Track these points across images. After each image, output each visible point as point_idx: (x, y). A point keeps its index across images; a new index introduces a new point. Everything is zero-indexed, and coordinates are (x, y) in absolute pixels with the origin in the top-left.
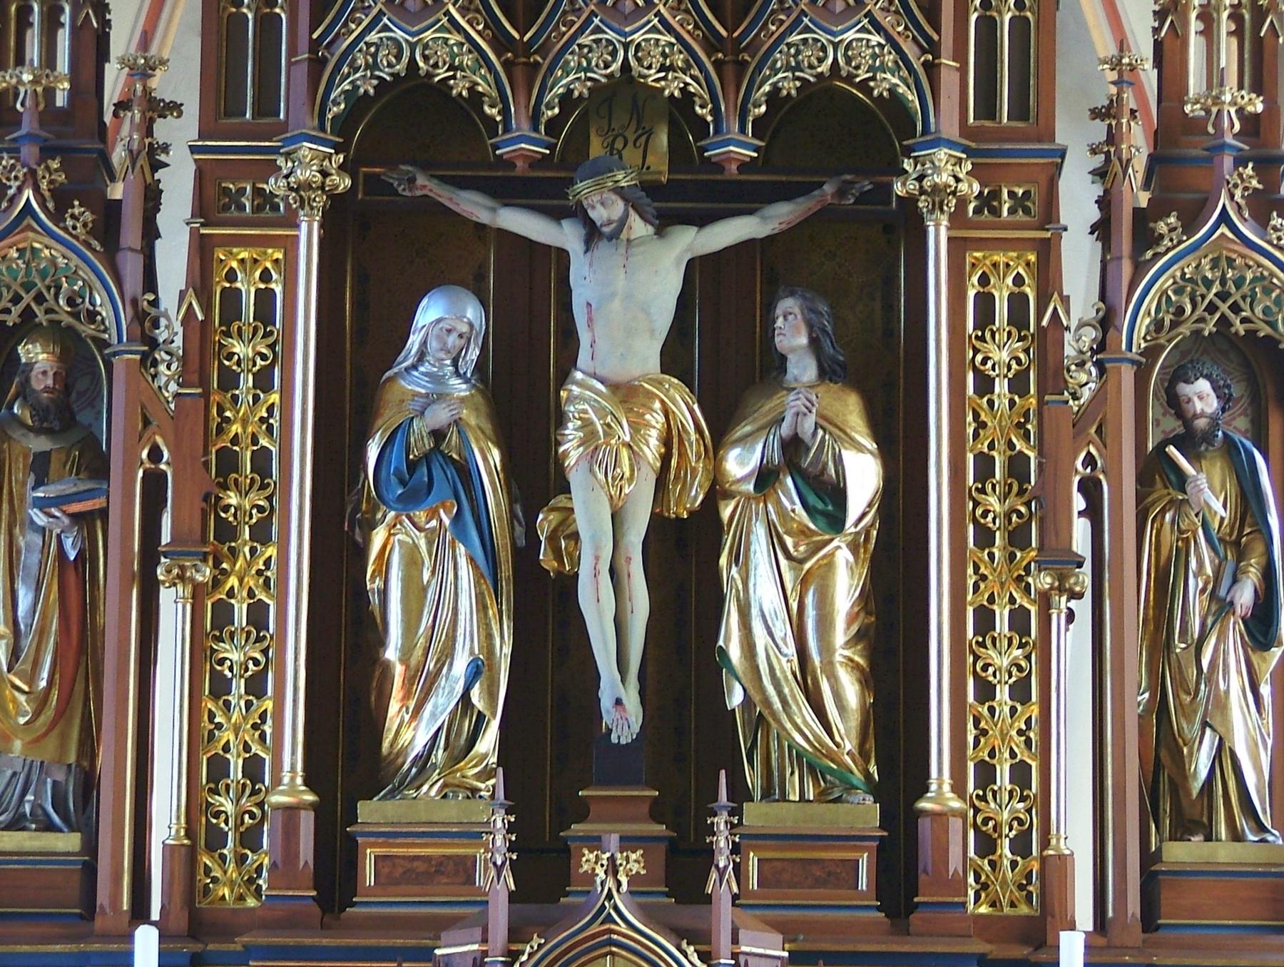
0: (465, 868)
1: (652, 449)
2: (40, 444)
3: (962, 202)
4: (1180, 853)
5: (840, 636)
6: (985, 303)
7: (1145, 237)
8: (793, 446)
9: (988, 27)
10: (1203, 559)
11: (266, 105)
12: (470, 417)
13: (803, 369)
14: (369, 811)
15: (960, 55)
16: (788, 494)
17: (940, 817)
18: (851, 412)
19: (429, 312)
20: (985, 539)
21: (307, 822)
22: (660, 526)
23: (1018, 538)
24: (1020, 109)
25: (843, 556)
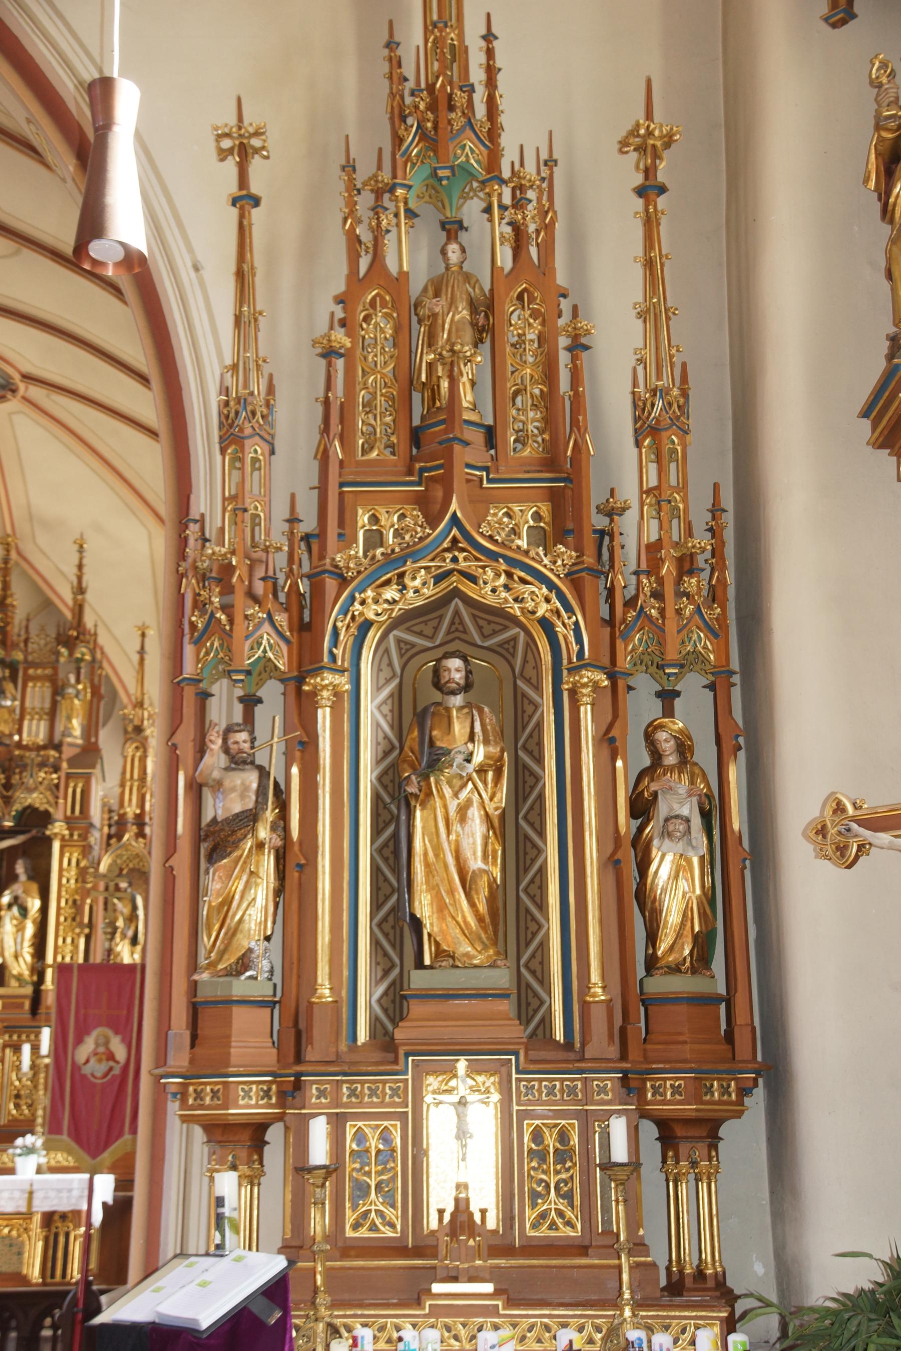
3: (63, 836)
7: (108, 845)
13: (23, 877)
15: (65, 798)
16: (15, 910)
18: (34, 887)
24: (81, 812)
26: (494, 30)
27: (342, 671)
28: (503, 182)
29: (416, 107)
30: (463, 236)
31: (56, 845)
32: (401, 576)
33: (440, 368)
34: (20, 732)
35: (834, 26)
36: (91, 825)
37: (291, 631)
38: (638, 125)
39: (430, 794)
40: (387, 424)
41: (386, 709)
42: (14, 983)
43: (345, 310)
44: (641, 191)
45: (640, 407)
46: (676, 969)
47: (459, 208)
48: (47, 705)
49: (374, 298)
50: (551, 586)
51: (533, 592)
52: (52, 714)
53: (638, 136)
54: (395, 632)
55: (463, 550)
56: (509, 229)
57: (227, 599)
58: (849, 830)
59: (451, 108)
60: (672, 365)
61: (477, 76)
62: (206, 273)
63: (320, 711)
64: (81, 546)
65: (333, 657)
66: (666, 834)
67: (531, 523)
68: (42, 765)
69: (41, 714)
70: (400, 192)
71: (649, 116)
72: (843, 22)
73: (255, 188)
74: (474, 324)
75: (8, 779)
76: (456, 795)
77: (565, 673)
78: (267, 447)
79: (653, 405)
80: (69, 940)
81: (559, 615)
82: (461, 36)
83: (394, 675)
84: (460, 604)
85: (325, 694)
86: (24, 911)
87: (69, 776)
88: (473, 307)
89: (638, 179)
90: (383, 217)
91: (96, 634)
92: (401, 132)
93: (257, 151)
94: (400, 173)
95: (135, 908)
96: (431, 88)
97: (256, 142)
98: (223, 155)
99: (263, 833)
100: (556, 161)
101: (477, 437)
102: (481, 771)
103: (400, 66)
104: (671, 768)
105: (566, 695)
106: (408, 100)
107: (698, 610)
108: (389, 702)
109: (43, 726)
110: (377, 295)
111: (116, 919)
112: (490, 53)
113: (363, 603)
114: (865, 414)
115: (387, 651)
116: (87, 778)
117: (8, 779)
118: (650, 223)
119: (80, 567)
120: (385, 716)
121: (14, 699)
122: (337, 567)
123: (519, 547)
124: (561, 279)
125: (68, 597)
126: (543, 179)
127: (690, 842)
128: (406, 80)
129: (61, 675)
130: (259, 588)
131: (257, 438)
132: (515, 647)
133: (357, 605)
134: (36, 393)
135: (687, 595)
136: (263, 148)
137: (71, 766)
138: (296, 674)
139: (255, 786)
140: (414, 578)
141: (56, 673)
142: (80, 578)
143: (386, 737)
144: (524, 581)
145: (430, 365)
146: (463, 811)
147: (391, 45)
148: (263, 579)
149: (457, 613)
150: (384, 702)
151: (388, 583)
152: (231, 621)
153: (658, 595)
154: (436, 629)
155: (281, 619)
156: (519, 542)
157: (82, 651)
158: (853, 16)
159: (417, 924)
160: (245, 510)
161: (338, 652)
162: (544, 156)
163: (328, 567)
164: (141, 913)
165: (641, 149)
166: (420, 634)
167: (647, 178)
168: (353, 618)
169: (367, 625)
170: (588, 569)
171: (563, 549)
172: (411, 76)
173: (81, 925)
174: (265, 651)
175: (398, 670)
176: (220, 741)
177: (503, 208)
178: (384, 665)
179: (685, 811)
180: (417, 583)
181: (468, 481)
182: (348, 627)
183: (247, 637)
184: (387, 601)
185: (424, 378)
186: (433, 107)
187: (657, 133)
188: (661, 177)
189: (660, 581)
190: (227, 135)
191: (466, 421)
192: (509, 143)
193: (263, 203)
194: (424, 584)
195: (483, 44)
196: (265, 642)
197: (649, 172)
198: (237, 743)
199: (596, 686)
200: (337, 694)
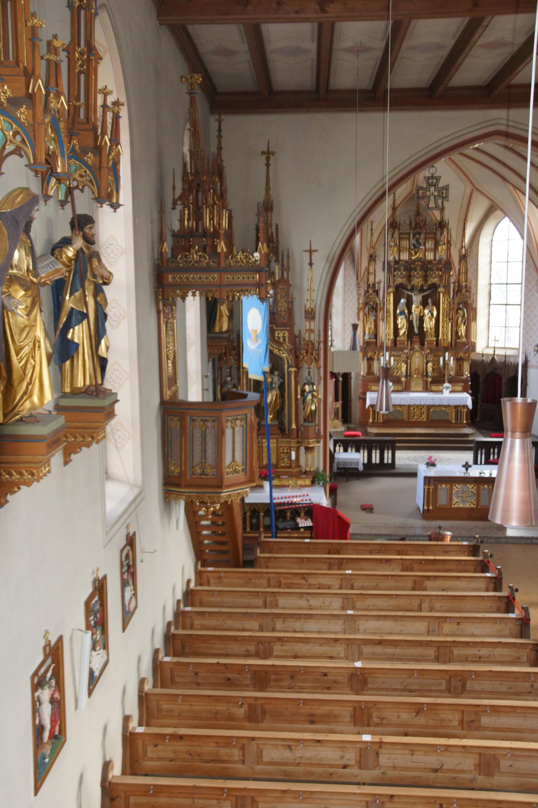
0: (405, 343)
4: (458, 341)
7: (457, 294)
8: (430, 311)
10: (460, 319)
12: (405, 308)
13: (430, 304)
14: (398, 339)
16: (430, 313)
17: (441, 340)
18: (435, 308)
19: (403, 301)
25: (434, 320)
31: (441, 295)
42: (430, 336)
48: (433, 247)
52: (435, 249)
68: (437, 270)
69: (430, 250)
75: (426, 274)
86: (432, 314)
87: (444, 272)
95: (464, 314)
111: (459, 317)
117: (426, 274)
129: (438, 238)
137: (445, 269)
164: (466, 315)
173: (449, 319)
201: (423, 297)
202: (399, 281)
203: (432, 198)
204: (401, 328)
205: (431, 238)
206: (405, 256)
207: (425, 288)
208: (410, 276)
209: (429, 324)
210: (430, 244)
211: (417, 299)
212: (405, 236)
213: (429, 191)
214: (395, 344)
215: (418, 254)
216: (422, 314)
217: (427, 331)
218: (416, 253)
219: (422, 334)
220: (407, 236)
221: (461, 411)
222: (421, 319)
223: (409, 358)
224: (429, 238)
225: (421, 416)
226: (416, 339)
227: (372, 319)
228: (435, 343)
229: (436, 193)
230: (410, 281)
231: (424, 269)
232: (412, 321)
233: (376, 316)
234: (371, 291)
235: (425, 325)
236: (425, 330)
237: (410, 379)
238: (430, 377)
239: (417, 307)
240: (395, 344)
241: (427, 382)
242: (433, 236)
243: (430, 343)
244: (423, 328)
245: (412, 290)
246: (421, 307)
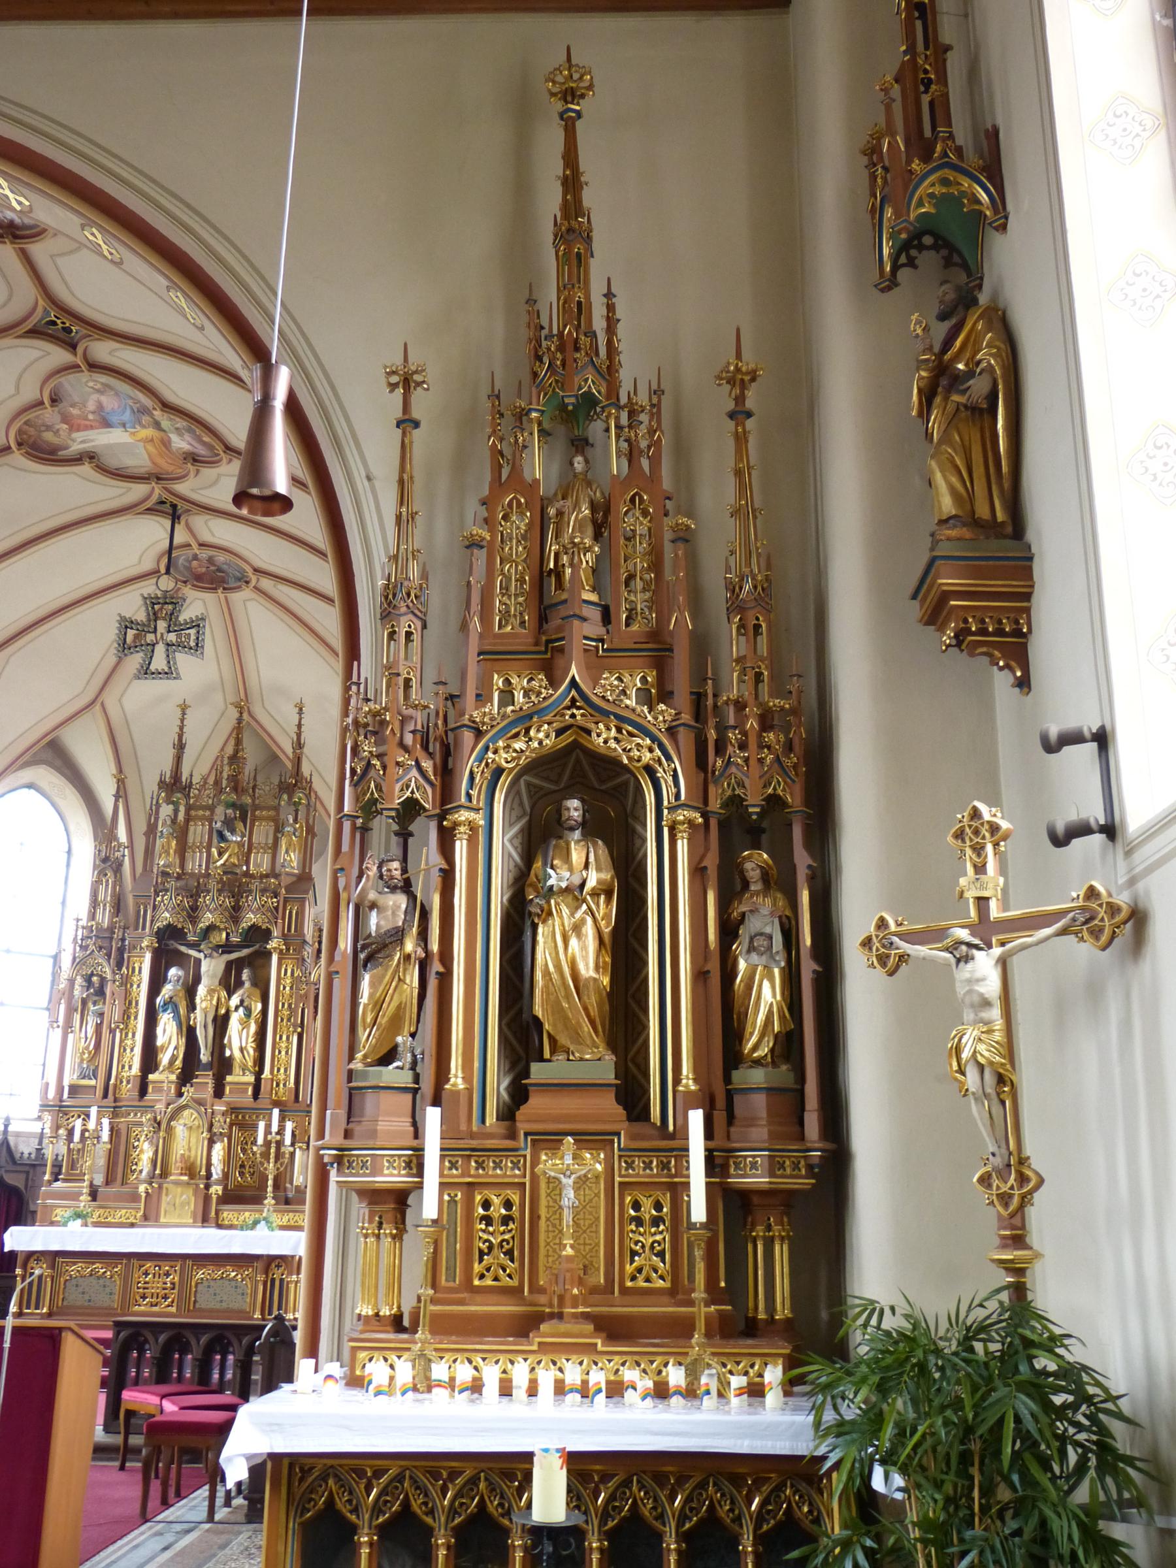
1: (214, 1002)
2: (96, 998)
3: (281, 950)
5: (251, 1040)
6: (286, 971)
8: (242, 1001)
9: (291, 913)
11: (144, 928)
13: (247, 985)
14: (151, 1077)
15: (284, 919)
16: (241, 1010)
18: (257, 992)
19: (173, 972)
20: (282, 1020)
21: (139, 1080)
22: (215, 1019)
23: (289, 1020)
24: (296, 930)
26: (613, 290)
27: (477, 810)
28: (620, 408)
29: (549, 349)
30: (588, 449)
31: (275, 958)
32: (527, 731)
33: (565, 557)
34: (247, 863)
35: (882, 290)
36: (305, 942)
37: (435, 775)
38: (729, 363)
39: (550, 914)
40: (520, 604)
41: (517, 842)
43: (487, 509)
44: (732, 415)
45: (733, 589)
46: (758, 1062)
47: (585, 429)
48: (270, 841)
49: (511, 501)
50: (654, 739)
51: (638, 744)
53: (728, 372)
54: (525, 777)
55: (579, 708)
56: (626, 445)
57: (382, 749)
58: (892, 943)
59: (577, 349)
60: (759, 555)
61: (599, 324)
62: (377, 484)
63: (458, 843)
64: (301, 709)
65: (469, 796)
66: (751, 949)
67: (639, 685)
68: (263, 891)
69: (265, 848)
70: (534, 415)
71: (739, 356)
72: (889, 288)
73: (416, 414)
74: (594, 521)
75: (237, 902)
76: (572, 915)
77: (666, 812)
78: (419, 624)
79: (741, 589)
80: (284, 1038)
81: (660, 764)
82: (588, 296)
83: (525, 814)
84: (582, 756)
85: (462, 829)
87: (286, 900)
88: (593, 507)
89: (731, 405)
90: (519, 435)
91: (311, 782)
92: (537, 368)
93: (419, 384)
94: (534, 400)
96: (561, 334)
97: (417, 378)
98: (393, 387)
99: (409, 946)
100: (663, 392)
101: (595, 614)
102: (595, 894)
103: (539, 317)
104: (757, 893)
105: (666, 831)
106: (544, 343)
107: (777, 759)
108: (520, 836)
109: (267, 858)
110: (514, 498)
112: (611, 308)
113: (495, 752)
114: (914, 597)
115: (518, 793)
116: (302, 901)
118: (741, 440)
119: (299, 726)
120: (516, 848)
121: (243, 836)
122: (474, 722)
123: (627, 707)
124: (667, 484)
125: (289, 751)
126: (653, 406)
127: (772, 957)
128: (542, 328)
129: (282, 816)
130: (409, 739)
131: (411, 616)
132: (626, 791)
133: (490, 755)
134: (266, 584)
135: (769, 747)
136: (424, 382)
137: (287, 892)
138: (438, 811)
139: (404, 906)
140: (538, 731)
141: (278, 814)
142: (299, 735)
143: (516, 865)
144: (631, 735)
145: (557, 555)
146: (577, 928)
147: (531, 301)
148: (413, 732)
149: (578, 761)
150: (516, 836)
151: (516, 735)
152: (384, 767)
153: (743, 746)
154: (560, 775)
155: (427, 765)
156: (628, 702)
157: (299, 795)
158: (897, 285)
159: (538, 1023)
160: (398, 675)
161: (474, 793)
162: (654, 386)
163: (467, 722)
165: (731, 381)
166: (547, 779)
167: (736, 405)
168: (487, 765)
169: (499, 772)
170: (683, 724)
171: (664, 708)
172: (545, 323)
173: (295, 1026)
174: (412, 792)
175: (528, 809)
176: (375, 868)
177: (619, 427)
178: (516, 806)
179: (768, 930)
180: (541, 735)
181: (586, 651)
182: (483, 772)
183: (398, 781)
184: (515, 751)
185: (552, 565)
186: (561, 348)
187: (744, 369)
188: (749, 404)
189: (745, 733)
190: (393, 373)
191: (585, 601)
192: (625, 376)
193: (422, 424)
194: (547, 736)
195: (605, 300)
196: (413, 784)
197: (740, 399)
198: (389, 870)
199: (690, 823)
200: (473, 827)
201: (229, 965)
202: (166, 917)
203: (160, 649)
204: (164, 1048)
205: (268, 819)
206: (196, 863)
207: (235, 939)
208: (195, 908)
209: (239, 1038)
210: (262, 832)
211: (211, 968)
212: (201, 813)
213: (155, 631)
214: (143, 1091)
215: (225, 857)
216: (223, 1011)
217: (231, 1058)
218: (220, 854)
219: (222, 1065)
220: (208, 813)
221: (282, 1280)
222: (221, 1023)
223: (163, 1126)
224: (261, 819)
225: (165, 1297)
226: (206, 1080)
227: (92, 1021)
228: (250, 1092)
229: (172, 637)
230: (194, 920)
231: (232, 892)
232: (195, 1029)
233: (101, 1015)
234: (92, 947)
235: (226, 1041)
236: (228, 1053)
237: (160, 1187)
238: (218, 1183)
239: (211, 992)
240: (143, 1091)
241: (207, 1199)
242: (272, 813)
243: (240, 1087)
244: (222, 1047)
245: (195, 946)
246: (224, 994)
